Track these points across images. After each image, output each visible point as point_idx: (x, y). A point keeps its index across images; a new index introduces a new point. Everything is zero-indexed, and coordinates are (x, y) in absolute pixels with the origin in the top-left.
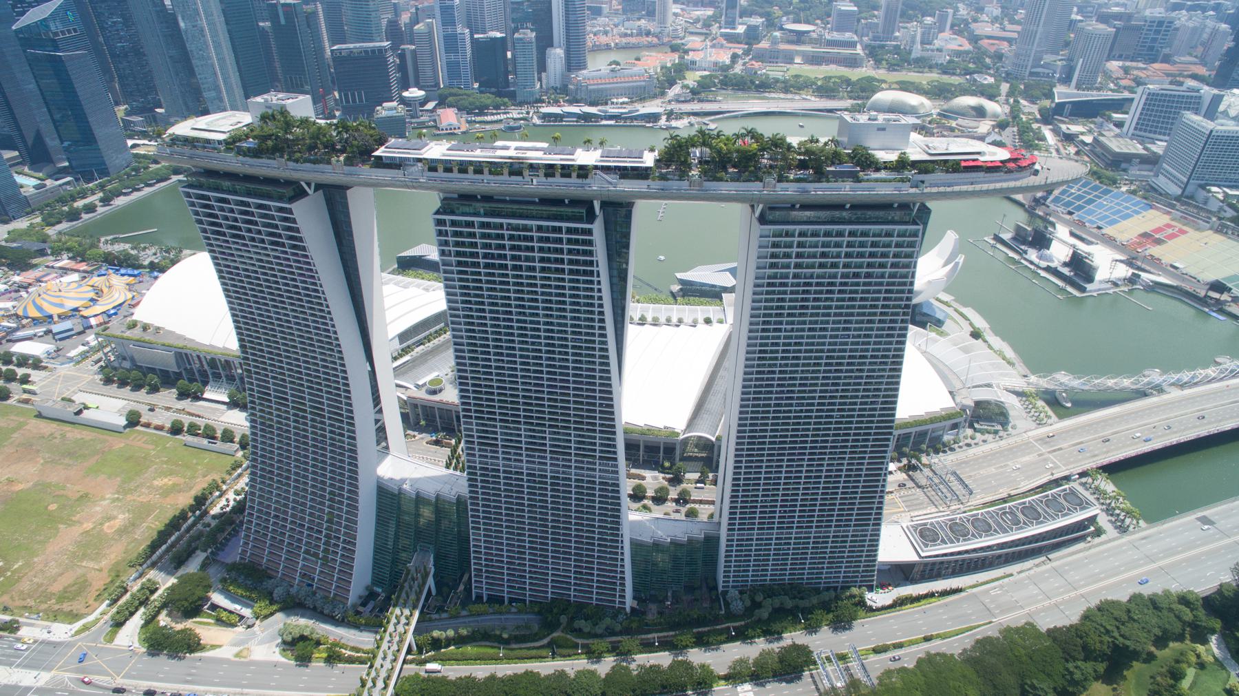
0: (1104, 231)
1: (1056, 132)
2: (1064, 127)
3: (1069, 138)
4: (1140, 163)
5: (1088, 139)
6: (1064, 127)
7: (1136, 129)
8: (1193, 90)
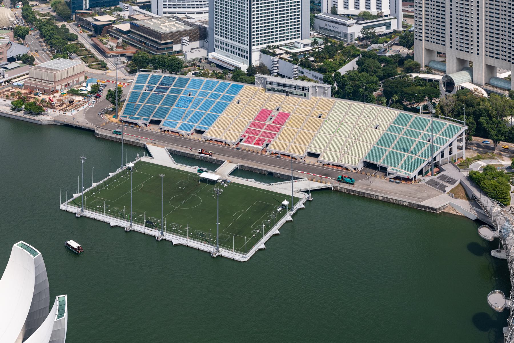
0: (208, 135)
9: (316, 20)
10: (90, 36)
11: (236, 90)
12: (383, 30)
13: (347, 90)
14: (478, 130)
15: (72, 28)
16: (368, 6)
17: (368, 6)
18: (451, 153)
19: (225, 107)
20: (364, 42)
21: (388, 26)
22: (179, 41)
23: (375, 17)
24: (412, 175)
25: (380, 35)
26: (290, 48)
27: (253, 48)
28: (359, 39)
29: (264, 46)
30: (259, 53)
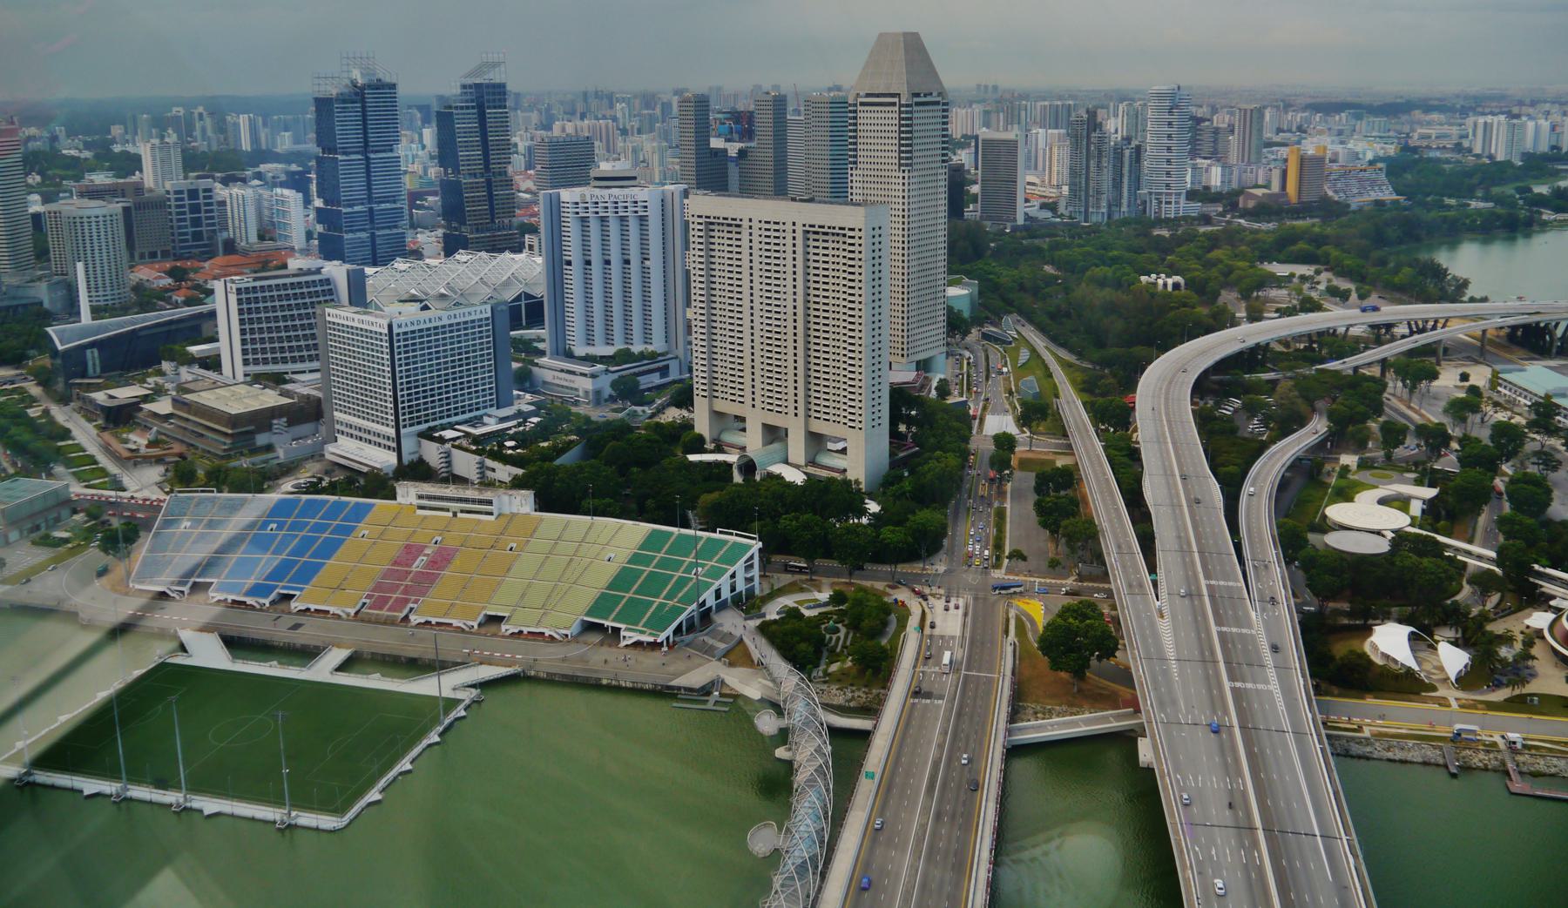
1: (90, 411)
2: (100, 397)
3: (119, 418)
4: (291, 423)
5: (163, 406)
6: (100, 397)
7: (246, 362)
8: (309, 272)
9: (535, 369)
10: (103, 429)
11: (359, 514)
12: (646, 382)
13: (556, 495)
14: (775, 546)
15: (60, 414)
16: (628, 338)
17: (628, 338)
18: (733, 589)
19: (337, 547)
20: (619, 404)
21: (664, 371)
22: (269, 428)
23: (642, 356)
24: (661, 638)
25: (649, 389)
26: (473, 426)
27: (403, 431)
28: (612, 399)
29: (424, 426)
30: (415, 439)
